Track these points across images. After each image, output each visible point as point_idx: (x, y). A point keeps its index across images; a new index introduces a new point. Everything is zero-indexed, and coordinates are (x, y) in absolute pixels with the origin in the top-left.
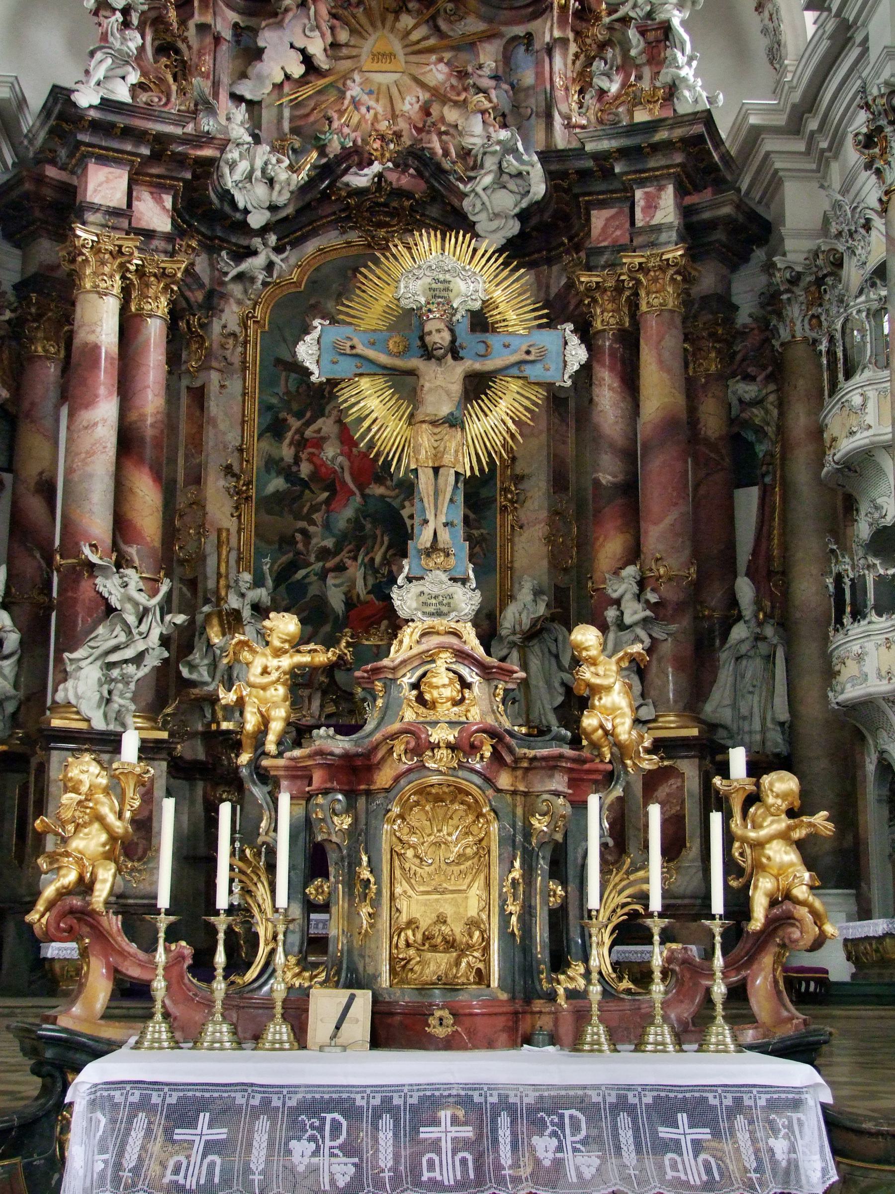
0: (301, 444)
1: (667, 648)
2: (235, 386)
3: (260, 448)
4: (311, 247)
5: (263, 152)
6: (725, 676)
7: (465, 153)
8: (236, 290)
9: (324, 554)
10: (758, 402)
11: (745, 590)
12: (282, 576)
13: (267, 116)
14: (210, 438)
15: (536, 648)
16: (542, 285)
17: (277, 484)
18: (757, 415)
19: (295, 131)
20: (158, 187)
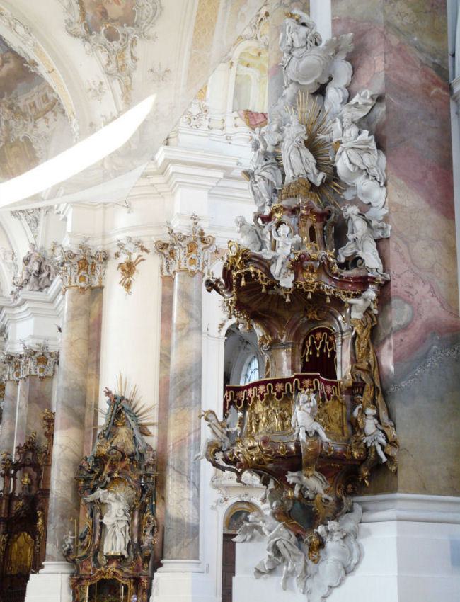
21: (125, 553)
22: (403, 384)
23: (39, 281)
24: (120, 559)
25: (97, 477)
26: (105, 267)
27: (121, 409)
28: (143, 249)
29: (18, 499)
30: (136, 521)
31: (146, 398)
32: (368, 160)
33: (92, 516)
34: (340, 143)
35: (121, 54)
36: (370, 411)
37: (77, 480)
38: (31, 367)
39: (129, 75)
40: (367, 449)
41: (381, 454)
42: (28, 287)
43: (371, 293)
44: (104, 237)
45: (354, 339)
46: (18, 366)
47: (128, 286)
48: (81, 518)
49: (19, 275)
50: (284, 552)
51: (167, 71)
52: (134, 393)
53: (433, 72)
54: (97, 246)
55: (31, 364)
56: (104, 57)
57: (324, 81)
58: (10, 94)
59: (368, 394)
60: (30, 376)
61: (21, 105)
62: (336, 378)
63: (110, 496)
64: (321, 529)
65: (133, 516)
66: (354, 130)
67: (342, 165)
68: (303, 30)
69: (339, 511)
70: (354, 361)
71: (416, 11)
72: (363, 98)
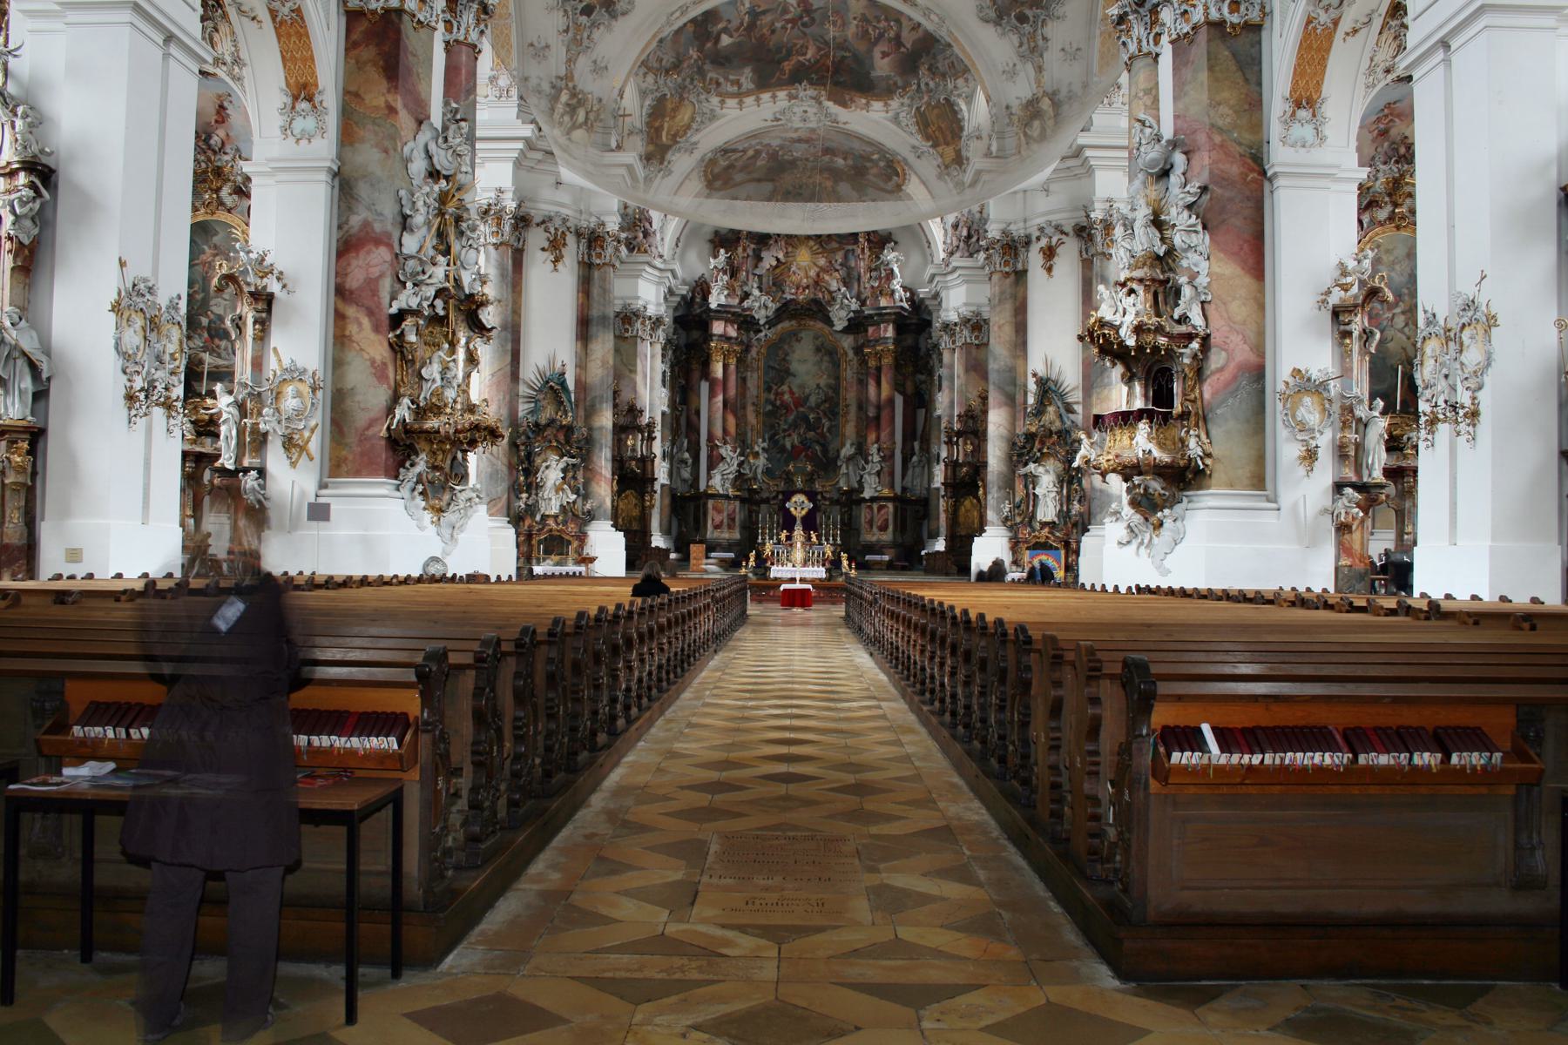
0: (777, 394)
1: (885, 470)
2: (755, 376)
3: (764, 396)
4: (779, 326)
5: (763, 298)
6: (910, 472)
7: (830, 293)
8: (755, 343)
9: (784, 431)
10: (925, 382)
11: (916, 445)
12: (771, 439)
13: (764, 280)
14: (748, 394)
15: (851, 463)
16: (856, 340)
17: (769, 408)
18: (924, 386)
19: (774, 284)
20: (732, 322)
21: (1056, 519)
22: (1218, 412)
23: (969, 246)
24: (1052, 525)
25: (1029, 452)
26: (1028, 251)
27: (1047, 389)
28: (1063, 232)
29: (962, 465)
30: (1065, 492)
31: (1070, 375)
32: (1194, 239)
33: (1026, 487)
34: (1174, 225)
35: (1033, 36)
36: (1192, 432)
37: (1010, 457)
38: (965, 335)
39: (1041, 56)
40: (1190, 460)
41: (1200, 463)
42: (958, 254)
43: (1195, 345)
44: (1025, 221)
45: (1184, 378)
46: (953, 335)
47: (1049, 270)
48: (1017, 489)
49: (949, 241)
50: (1135, 530)
51: (1078, 49)
52: (1060, 373)
53: (1250, 161)
54: (1017, 230)
55: (966, 332)
56: (1015, 39)
57: (1168, 167)
58: (928, 53)
59: (1193, 419)
60: (965, 344)
61: (939, 65)
62: (1172, 407)
63: (1041, 469)
64: (1159, 514)
65: (1062, 487)
66: (1186, 213)
67: (1177, 241)
68: (1148, 131)
69: (1172, 502)
70: (1184, 394)
71: (1235, 112)
72: (1193, 187)
